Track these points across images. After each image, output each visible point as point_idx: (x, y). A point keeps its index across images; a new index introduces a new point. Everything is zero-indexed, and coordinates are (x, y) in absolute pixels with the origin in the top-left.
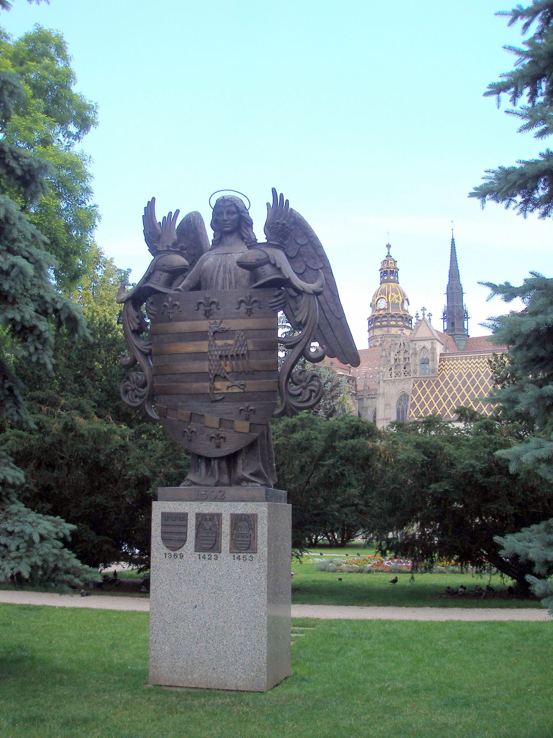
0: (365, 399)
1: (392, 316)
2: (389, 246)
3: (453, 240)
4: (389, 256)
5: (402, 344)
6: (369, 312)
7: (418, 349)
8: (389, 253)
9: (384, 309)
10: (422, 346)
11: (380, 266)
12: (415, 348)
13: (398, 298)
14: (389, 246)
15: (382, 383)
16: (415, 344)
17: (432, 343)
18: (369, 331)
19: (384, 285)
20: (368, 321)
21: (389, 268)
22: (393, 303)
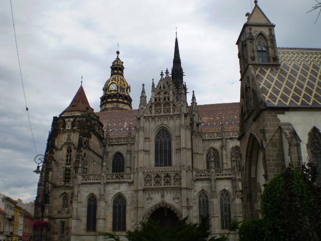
0: (107, 145)
1: (121, 96)
2: (118, 53)
3: (176, 39)
4: (118, 58)
5: (162, 86)
6: (102, 94)
7: (254, 35)
8: (118, 57)
9: (115, 91)
10: (258, 33)
11: (111, 65)
12: (251, 33)
13: (124, 85)
14: (118, 53)
15: (142, 119)
16: (250, 29)
17: (270, 30)
18: (100, 106)
19: (114, 76)
20: (100, 100)
21: (118, 65)
22: (121, 88)
